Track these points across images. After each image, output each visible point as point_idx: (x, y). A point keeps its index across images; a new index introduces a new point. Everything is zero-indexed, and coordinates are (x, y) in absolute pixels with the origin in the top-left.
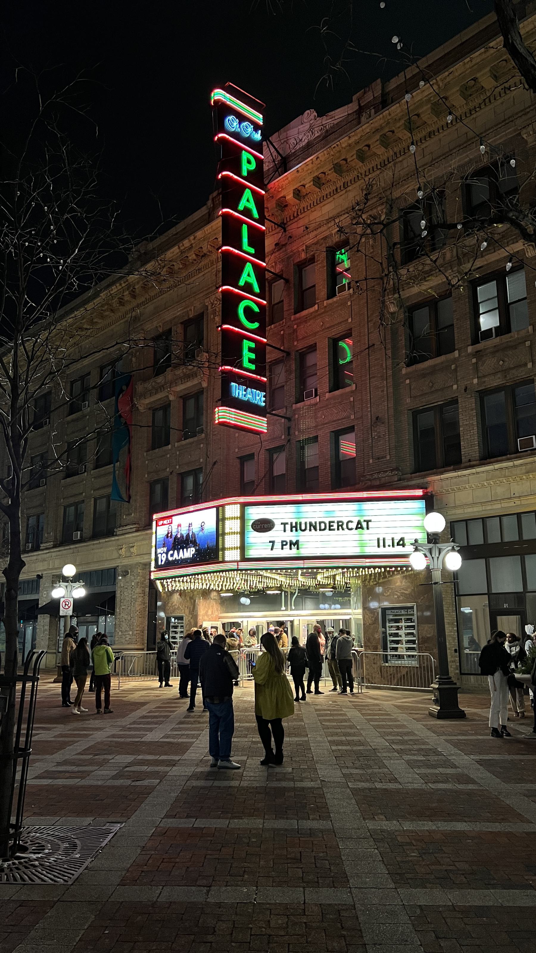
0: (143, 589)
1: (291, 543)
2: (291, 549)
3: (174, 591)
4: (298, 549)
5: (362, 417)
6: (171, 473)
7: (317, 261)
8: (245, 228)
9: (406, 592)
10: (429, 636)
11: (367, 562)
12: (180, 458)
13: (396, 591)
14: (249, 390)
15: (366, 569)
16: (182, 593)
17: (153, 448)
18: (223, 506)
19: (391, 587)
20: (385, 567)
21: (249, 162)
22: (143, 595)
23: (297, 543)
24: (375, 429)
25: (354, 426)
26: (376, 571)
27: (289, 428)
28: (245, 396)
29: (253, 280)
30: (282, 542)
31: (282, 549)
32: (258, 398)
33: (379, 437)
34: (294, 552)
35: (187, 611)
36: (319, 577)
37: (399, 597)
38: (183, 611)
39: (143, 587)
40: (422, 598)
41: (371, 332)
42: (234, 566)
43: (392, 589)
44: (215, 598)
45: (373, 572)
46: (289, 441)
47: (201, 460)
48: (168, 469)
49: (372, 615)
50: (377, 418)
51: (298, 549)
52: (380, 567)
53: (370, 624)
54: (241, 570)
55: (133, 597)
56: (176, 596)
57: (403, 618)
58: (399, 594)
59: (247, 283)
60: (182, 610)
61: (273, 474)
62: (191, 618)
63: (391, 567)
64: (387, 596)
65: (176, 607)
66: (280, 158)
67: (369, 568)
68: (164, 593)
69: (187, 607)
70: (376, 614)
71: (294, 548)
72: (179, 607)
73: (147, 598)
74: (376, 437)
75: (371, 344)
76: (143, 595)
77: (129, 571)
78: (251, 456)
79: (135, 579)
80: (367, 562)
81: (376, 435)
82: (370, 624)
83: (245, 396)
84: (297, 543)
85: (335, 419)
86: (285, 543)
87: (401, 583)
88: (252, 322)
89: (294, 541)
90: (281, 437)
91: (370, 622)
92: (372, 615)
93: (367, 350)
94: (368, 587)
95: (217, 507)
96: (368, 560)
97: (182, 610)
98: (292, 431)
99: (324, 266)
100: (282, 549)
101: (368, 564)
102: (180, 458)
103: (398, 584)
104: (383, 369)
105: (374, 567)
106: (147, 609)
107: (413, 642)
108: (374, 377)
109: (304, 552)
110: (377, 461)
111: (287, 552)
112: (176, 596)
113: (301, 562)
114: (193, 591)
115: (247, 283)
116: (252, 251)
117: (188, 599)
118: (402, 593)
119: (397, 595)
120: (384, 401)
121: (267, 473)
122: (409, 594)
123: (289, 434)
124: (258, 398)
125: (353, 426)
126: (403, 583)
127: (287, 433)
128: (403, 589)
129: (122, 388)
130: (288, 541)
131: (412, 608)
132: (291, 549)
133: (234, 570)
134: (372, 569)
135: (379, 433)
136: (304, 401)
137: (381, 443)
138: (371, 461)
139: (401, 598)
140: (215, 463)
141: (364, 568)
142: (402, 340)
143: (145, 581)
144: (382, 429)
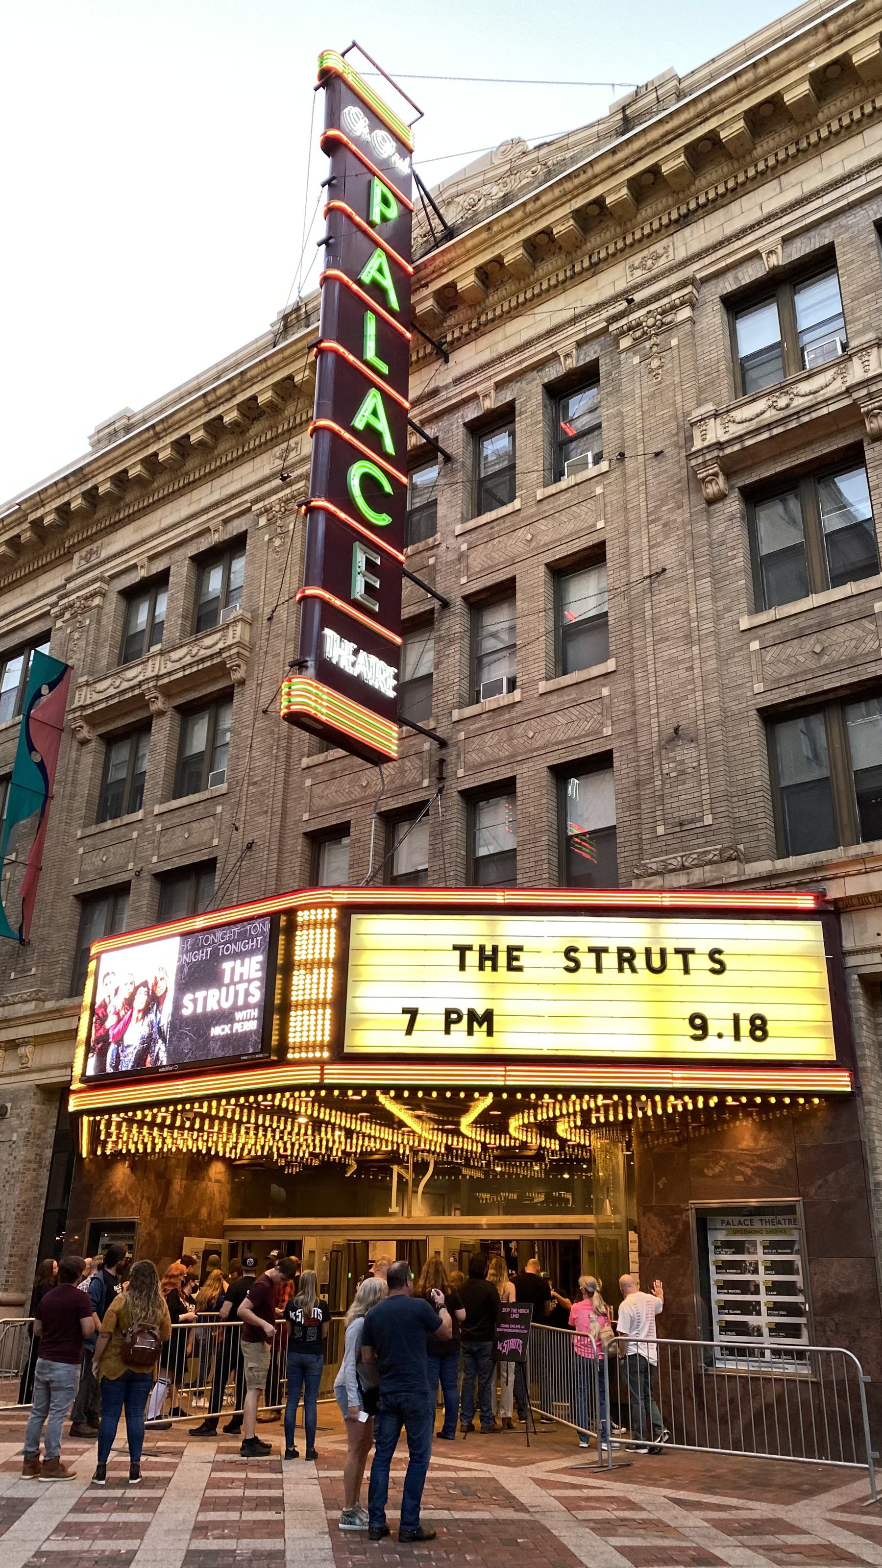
0: (39, 1151)
1: (472, 1015)
2: (470, 1032)
3: (117, 1155)
4: (490, 1033)
5: (633, 731)
6: (138, 874)
7: (521, 414)
8: (370, 316)
9: (769, 1166)
10: (843, 1290)
11: (678, 1079)
12: (163, 839)
13: (741, 1164)
14: (363, 654)
15: (658, 1098)
16: (139, 1162)
17: (101, 819)
18: (291, 913)
19: (726, 1151)
20: (722, 1094)
21: (385, 201)
22: (35, 1166)
23: (488, 1016)
24: (672, 755)
25: (611, 750)
26: (700, 1105)
27: (442, 762)
28: (353, 665)
29: (382, 425)
30: (448, 1012)
31: (447, 1031)
32: (380, 676)
33: (683, 773)
34: (478, 1043)
35: (146, 1208)
36: (514, 1123)
37: (748, 1179)
38: (136, 1208)
39: (38, 1146)
40: (820, 1182)
41: (658, 544)
42: (310, 1075)
43: (727, 1157)
44: (219, 1177)
45: (690, 1107)
46: (440, 791)
47: (215, 842)
48: (131, 866)
49: (669, 1230)
50: (676, 730)
51: (490, 1033)
52: (707, 1093)
53: (662, 1255)
54: (330, 1088)
55: (13, 1170)
56: (121, 1172)
57: (759, 1239)
58: (749, 1172)
59: (369, 427)
60: (132, 1206)
61: (392, 873)
62: (156, 1227)
63: (736, 1094)
64: (714, 1177)
65: (119, 1197)
66: (442, 227)
67: (679, 1093)
68: (91, 1160)
69: (148, 1199)
70: (680, 1226)
71: (480, 1031)
72: (126, 1196)
73: (45, 1174)
74: (672, 775)
75: (656, 568)
76: (35, 1166)
77: (9, 1105)
78: (341, 831)
79: (21, 1126)
80: (678, 1079)
81: (674, 769)
82: (662, 1255)
83: (353, 665)
84: (488, 1016)
85: (561, 737)
86: (454, 1016)
87: (756, 1139)
88: (378, 510)
89: (480, 1012)
90: (421, 782)
91: (663, 1247)
92: (669, 1230)
93: (647, 581)
94: (656, 1150)
95: (274, 916)
96: (678, 1073)
97: (132, 1206)
98: (448, 771)
99: (538, 423)
100: (447, 1031)
101: (678, 1084)
102: (163, 839)
103: (747, 1142)
104: (690, 622)
105: (693, 1093)
106: (43, 1202)
107: (793, 1310)
108: (667, 639)
109: (505, 1042)
110: (678, 829)
111: (460, 1041)
112: (121, 1172)
113: (499, 1070)
114: (165, 1157)
115: (369, 427)
116: (385, 369)
117: (153, 1178)
118: (759, 1168)
119: (742, 1173)
120: (694, 691)
121: (379, 870)
122: (779, 1172)
123: (441, 779)
124: (379, 676)
125: (610, 752)
126: (762, 1143)
127: (435, 774)
128: (760, 1157)
129: (40, 690)
130: (465, 1012)
131: (790, 1209)
132: (470, 1032)
133: (307, 1088)
134: (686, 1098)
135: (682, 762)
136: (478, 702)
137: (686, 786)
138: (661, 830)
139: (757, 1183)
140: (250, 846)
141: (665, 1093)
142: (734, 557)
143: (45, 1131)
144: (687, 754)
